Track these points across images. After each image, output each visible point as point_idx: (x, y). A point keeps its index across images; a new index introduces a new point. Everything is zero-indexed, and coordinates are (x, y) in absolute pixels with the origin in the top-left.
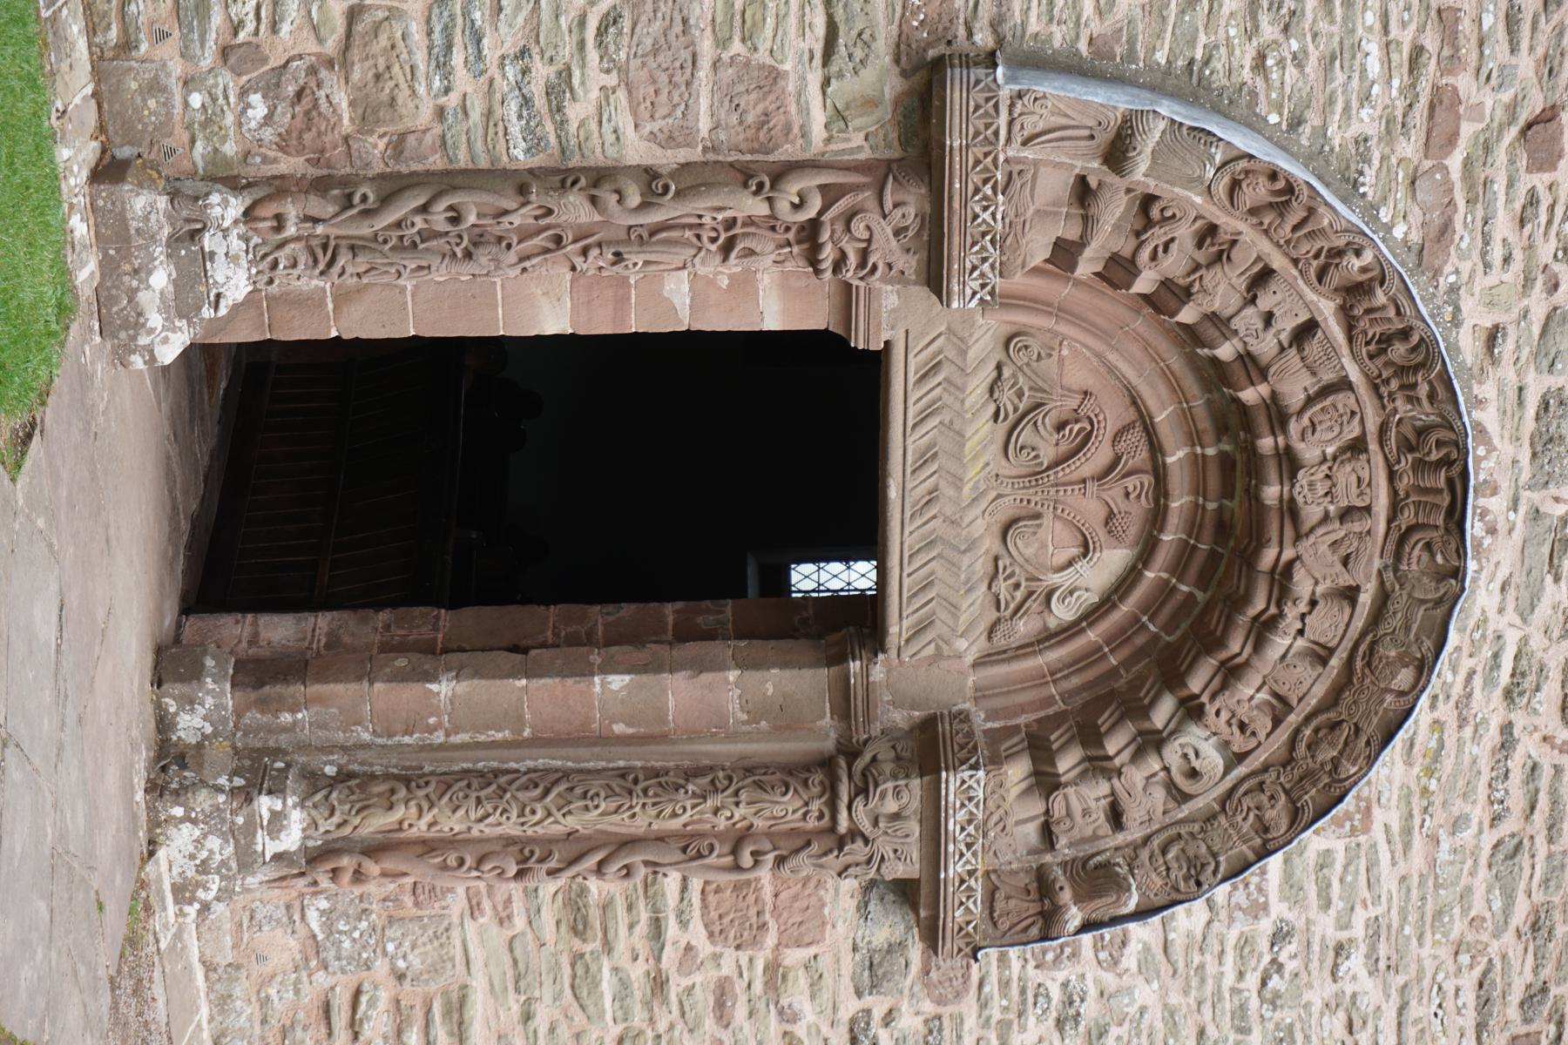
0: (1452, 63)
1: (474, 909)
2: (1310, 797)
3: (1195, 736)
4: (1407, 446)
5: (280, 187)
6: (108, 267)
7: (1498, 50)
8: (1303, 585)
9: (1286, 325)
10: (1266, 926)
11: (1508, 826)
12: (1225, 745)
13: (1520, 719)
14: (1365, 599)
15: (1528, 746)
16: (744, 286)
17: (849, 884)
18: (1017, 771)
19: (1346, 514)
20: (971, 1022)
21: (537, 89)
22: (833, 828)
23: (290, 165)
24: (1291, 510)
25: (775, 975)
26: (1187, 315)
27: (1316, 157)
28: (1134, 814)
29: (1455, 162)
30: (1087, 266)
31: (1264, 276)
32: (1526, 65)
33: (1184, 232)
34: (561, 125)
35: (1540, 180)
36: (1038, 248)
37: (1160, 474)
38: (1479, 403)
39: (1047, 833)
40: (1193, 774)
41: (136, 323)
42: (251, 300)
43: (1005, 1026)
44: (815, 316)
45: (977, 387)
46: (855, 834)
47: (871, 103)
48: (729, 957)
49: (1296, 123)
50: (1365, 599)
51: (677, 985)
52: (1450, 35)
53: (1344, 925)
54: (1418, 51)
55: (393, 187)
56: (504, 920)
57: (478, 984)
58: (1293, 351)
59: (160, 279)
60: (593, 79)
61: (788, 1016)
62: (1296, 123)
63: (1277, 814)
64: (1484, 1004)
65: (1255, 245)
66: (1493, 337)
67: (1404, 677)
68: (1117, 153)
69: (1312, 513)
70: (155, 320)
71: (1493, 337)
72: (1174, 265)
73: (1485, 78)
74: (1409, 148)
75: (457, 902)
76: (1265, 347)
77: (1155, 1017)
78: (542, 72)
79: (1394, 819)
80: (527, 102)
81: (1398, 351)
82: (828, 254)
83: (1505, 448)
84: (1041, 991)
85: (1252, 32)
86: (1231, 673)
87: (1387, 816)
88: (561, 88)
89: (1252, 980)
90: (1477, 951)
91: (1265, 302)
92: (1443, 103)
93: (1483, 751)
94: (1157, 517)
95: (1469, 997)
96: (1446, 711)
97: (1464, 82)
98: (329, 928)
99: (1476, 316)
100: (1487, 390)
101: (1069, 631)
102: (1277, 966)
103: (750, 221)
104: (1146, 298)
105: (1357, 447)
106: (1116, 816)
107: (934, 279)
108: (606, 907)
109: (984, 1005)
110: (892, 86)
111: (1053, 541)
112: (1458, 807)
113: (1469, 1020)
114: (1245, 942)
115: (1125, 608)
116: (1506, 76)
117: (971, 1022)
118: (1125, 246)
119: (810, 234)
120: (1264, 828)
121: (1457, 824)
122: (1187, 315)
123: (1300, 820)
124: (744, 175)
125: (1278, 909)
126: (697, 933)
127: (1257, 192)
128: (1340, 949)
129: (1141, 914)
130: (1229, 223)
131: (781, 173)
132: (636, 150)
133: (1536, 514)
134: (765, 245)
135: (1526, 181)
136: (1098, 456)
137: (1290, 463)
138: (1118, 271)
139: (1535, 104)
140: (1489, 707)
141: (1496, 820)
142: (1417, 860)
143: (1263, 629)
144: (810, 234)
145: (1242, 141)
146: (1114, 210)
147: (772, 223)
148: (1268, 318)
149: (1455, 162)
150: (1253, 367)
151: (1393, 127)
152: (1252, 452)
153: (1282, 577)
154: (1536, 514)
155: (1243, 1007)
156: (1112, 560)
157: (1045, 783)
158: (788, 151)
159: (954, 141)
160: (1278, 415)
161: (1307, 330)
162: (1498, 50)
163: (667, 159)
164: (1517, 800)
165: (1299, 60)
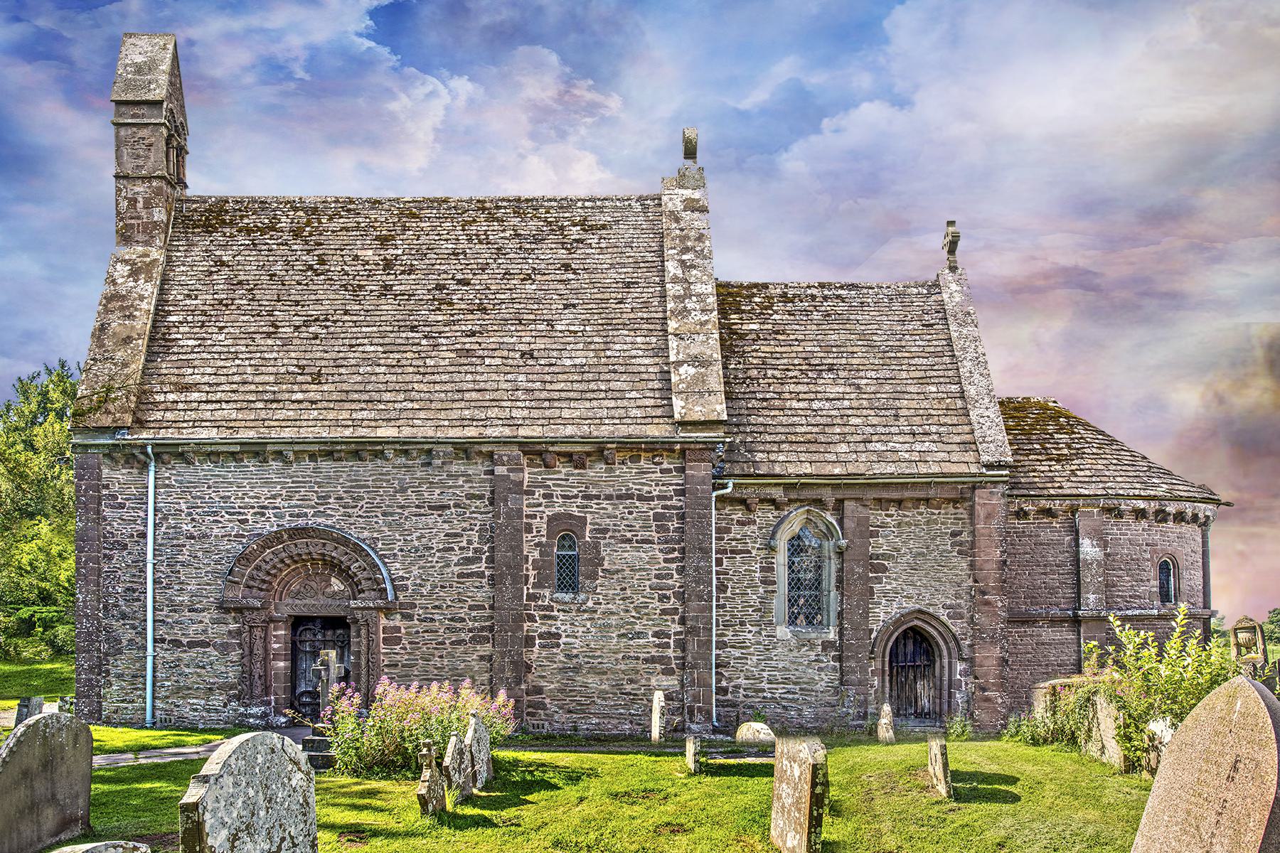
11: (379, 515)
15: (360, 513)
51: (409, 650)
52: (225, 536)
64: (420, 515)
66: (278, 525)
71: (278, 525)
74: (244, 541)
77: (421, 571)
87: (375, 535)
92: (235, 536)
96: (352, 527)
116: (232, 528)
126: (398, 647)
141: (377, 516)
151: (241, 543)
164: (373, 514)
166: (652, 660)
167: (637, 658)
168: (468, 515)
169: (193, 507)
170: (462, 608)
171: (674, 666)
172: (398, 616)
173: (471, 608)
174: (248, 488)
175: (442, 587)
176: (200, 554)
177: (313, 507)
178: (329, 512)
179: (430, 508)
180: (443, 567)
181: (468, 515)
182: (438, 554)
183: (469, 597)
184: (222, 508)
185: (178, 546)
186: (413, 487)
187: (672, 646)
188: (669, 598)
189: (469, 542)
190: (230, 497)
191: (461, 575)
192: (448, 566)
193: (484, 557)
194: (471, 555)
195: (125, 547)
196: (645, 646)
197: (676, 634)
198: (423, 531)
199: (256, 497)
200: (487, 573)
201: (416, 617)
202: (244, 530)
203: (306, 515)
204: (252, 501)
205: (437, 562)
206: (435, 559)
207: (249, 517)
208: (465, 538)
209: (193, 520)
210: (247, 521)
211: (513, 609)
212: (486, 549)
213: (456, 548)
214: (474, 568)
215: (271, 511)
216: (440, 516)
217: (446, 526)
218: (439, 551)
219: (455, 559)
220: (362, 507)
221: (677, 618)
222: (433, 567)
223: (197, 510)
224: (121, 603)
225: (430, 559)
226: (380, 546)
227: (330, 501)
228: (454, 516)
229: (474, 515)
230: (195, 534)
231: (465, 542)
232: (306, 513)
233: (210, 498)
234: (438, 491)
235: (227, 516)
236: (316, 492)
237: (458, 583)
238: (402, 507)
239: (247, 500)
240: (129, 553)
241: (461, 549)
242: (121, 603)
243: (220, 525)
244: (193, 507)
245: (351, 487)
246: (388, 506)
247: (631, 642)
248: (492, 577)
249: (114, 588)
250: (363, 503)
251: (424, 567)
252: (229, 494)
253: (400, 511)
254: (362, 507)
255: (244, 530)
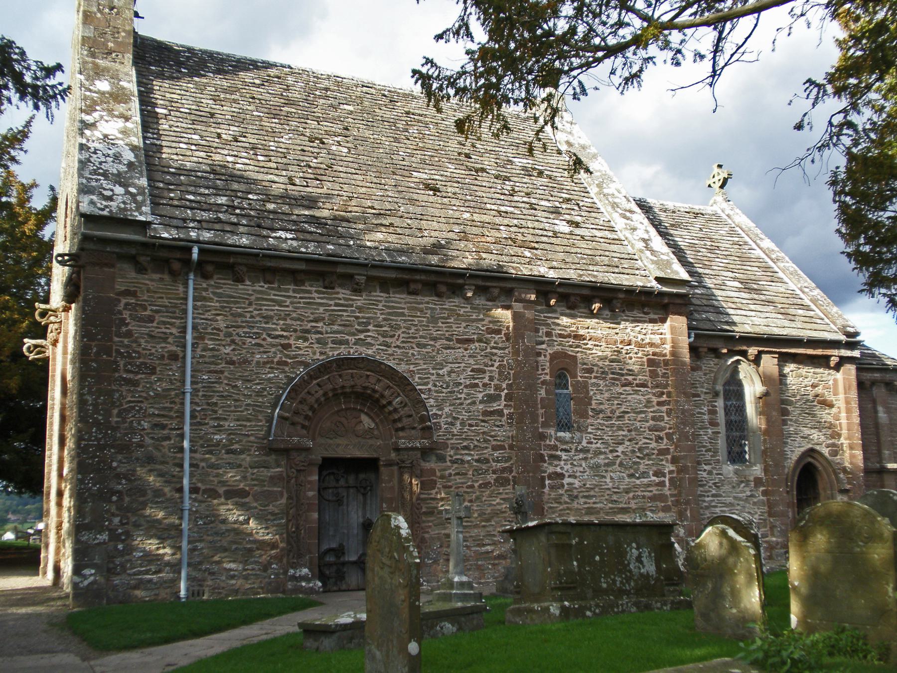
0: (272, 362)
1: (428, 532)
2: (406, 382)
3: (394, 403)
4: (340, 367)
5: (288, 562)
6: (301, 592)
7: (270, 354)
8: (367, 384)
9: (318, 388)
10: (433, 388)
11: (414, 346)
12: (397, 397)
13: (393, 345)
14: (368, 373)
15: (398, 343)
16: (310, 482)
17: (423, 464)
18: (401, 434)
19: (352, 377)
20: (452, 441)
21: (272, 518)
22: (411, 467)
23: (285, 560)
24: (352, 387)
25: (442, 477)
26: (316, 406)
27: (288, 384)
28: (410, 413)
29: (289, 361)
30: (307, 424)
31: (309, 393)
32: (273, 350)
33: (300, 406)
34: (278, 514)
35: (293, 346)
36: (305, 432)
37: (347, 409)
38: (333, 355)
39: (414, 428)
40: (402, 403)
41: (312, 588)
42: (310, 570)
43: (453, 435)
44: (316, 470)
45: (331, 441)
46: (411, 463)
47: (276, 461)
48: (438, 486)
49: (281, 388)
50: (368, 373)
52: (268, 363)
53: (433, 374)
54: (270, 368)
55: (288, 543)
56: (430, 527)
57: (443, 532)
58: (324, 387)
59: (304, 584)
60: (271, 508)
61: (450, 475)
62: (281, 388)
63: (409, 388)
65: (303, 394)
67: (383, 367)
68: (286, 419)
69: (352, 383)
70: (311, 585)
71: (321, 353)
72: (306, 408)
73: (275, 357)
74: (287, 369)
75: (426, 536)
76: (321, 392)
77: (452, 408)
78: (269, 517)
79: (412, 366)
80: (274, 520)
81: (322, 370)
82: (302, 468)
83: (342, 350)
84: (446, 429)
85: (265, 396)
86: (382, 396)
87: (412, 367)
88: (272, 514)
89: (444, 390)
90: (438, 350)
91: (313, 392)
92: (279, 363)
93: (399, 351)
94: (355, 409)
95: (448, 351)
96: (391, 358)
97: (275, 360)
98: (431, 559)
99: (317, 356)
100: (331, 353)
101: (376, 424)
102: (441, 386)
103: (296, 481)
104: (313, 412)
105: (340, 376)
106: (410, 416)
107: (308, 450)
108: (427, 508)
109: (448, 439)
110: (273, 457)
111: (359, 428)
112: (410, 355)
113: (453, 351)
114: (437, 392)
115: (372, 415)
116: (275, 353)
117: (452, 441)
118: (302, 417)
119: (299, 471)
120: (411, 390)
121: (413, 355)
122: (316, 406)
123: (410, 384)
124: (288, 482)
125: (430, 386)
126: (434, 491)
127: (293, 395)
128: (438, 374)
129: (428, 412)
130: (299, 399)
131: (288, 476)
132: (284, 501)
133: (355, 344)
134: (302, 478)
135: (293, 349)
136: (343, 420)
137: (343, 387)
138: (307, 417)
139: (280, 347)
140: (390, 351)
141: (413, 348)
142: (421, 362)
143: (374, 391)
144: (299, 471)
145: (283, 398)
146: (298, 419)
147: (296, 478)
148: (316, 392)
149: (289, 361)
150: (325, 394)
151: (284, 372)
152: (342, 394)
153: (365, 388)
154: (355, 344)
155: (450, 392)
156: (364, 418)
157: (402, 429)
158: (284, 474)
159: (282, 446)
160: (334, 389)
161: (318, 385)
162: (270, 354)
163: (285, 496)
164: (409, 345)
165: (270, 388)
166: (653, 498)
167: (644, 497)
168: (488, 350)
169: (232, 326)
170: (487, 448)
171: (670, 503)
172: (434, 458)
173: (495, 448)
174: (290, 309)
175: (470, 425)
176: (239, 383)
177: (354, 334)
178: (369, 340)
179: (459, 341)
180: (469, 404)
181: (488, 350)
182: (465, 390)
183: (491, 436)
184: (264, 329)
185: (216, 372)
186: (443, 318)
187: (667, 484)
188: (662, 439)
189: (491, 379)
190: (271, 317)
191: (486, 413)
192: (474, 403)
193: (503, 394)
194: (492, 392)
195: (153, 371)
196: (649, 485)
197: (671, 472)
198: (453, 365)
199: (299, 319)
200: (506, 412)
201: (448, 458)
202: (287, 356)
203: (347, 342)
204: (294, 323)
205: (465, 399)
206: (463, 396)
207: (292, 342)
208: (488, 374)
209: (233, 342)
210: (290, 345)
211: (532, 449)
212: (504, 386)
213: (480, 385)
214: (495, 406)
215: (314, 336)
216: (466, 349)
217: (472, 361)
218: (466, 387)
219: (480, 396)
220: (399, 336)
221: (669, 457)
222: (461, 404)
223: (240, 331)
224: (148, 441)
225: (459, 396)
226: (417, 380)
227: (370, 327)
228: (478, 351)
229: (494, 351)
230: (235, 358)
231: (487, 378)
232: (348, 340)
233: (252, 317)
234: (464, 324)
235: (269, 340)
236: (357, 318)
237: (483, 421)
238: (435, 339)
239: (289, 322)
240: (159, 380)
241: (485, 385)
242: (148, 441)
243: (262, 349)
244: (232, 326)
245: (389, 314)
246: (421, 337)
247: (638, 482)
248: (510, 416)
249: (139, 424)
250: (400, 332)
251: (454, 405)
252: (272, 313)
253: (432, 343)
254: (399, 336)
255: (287, 356)
